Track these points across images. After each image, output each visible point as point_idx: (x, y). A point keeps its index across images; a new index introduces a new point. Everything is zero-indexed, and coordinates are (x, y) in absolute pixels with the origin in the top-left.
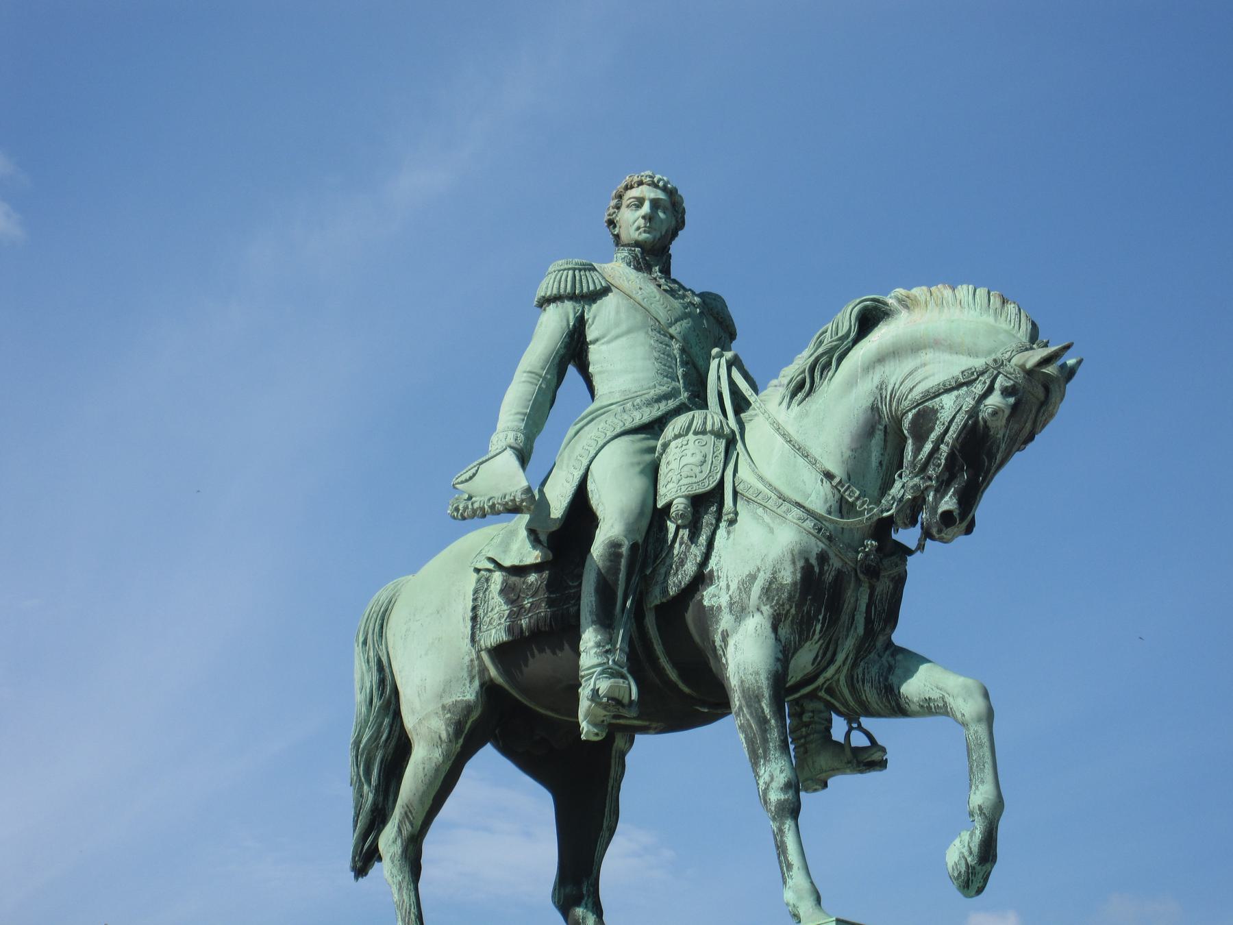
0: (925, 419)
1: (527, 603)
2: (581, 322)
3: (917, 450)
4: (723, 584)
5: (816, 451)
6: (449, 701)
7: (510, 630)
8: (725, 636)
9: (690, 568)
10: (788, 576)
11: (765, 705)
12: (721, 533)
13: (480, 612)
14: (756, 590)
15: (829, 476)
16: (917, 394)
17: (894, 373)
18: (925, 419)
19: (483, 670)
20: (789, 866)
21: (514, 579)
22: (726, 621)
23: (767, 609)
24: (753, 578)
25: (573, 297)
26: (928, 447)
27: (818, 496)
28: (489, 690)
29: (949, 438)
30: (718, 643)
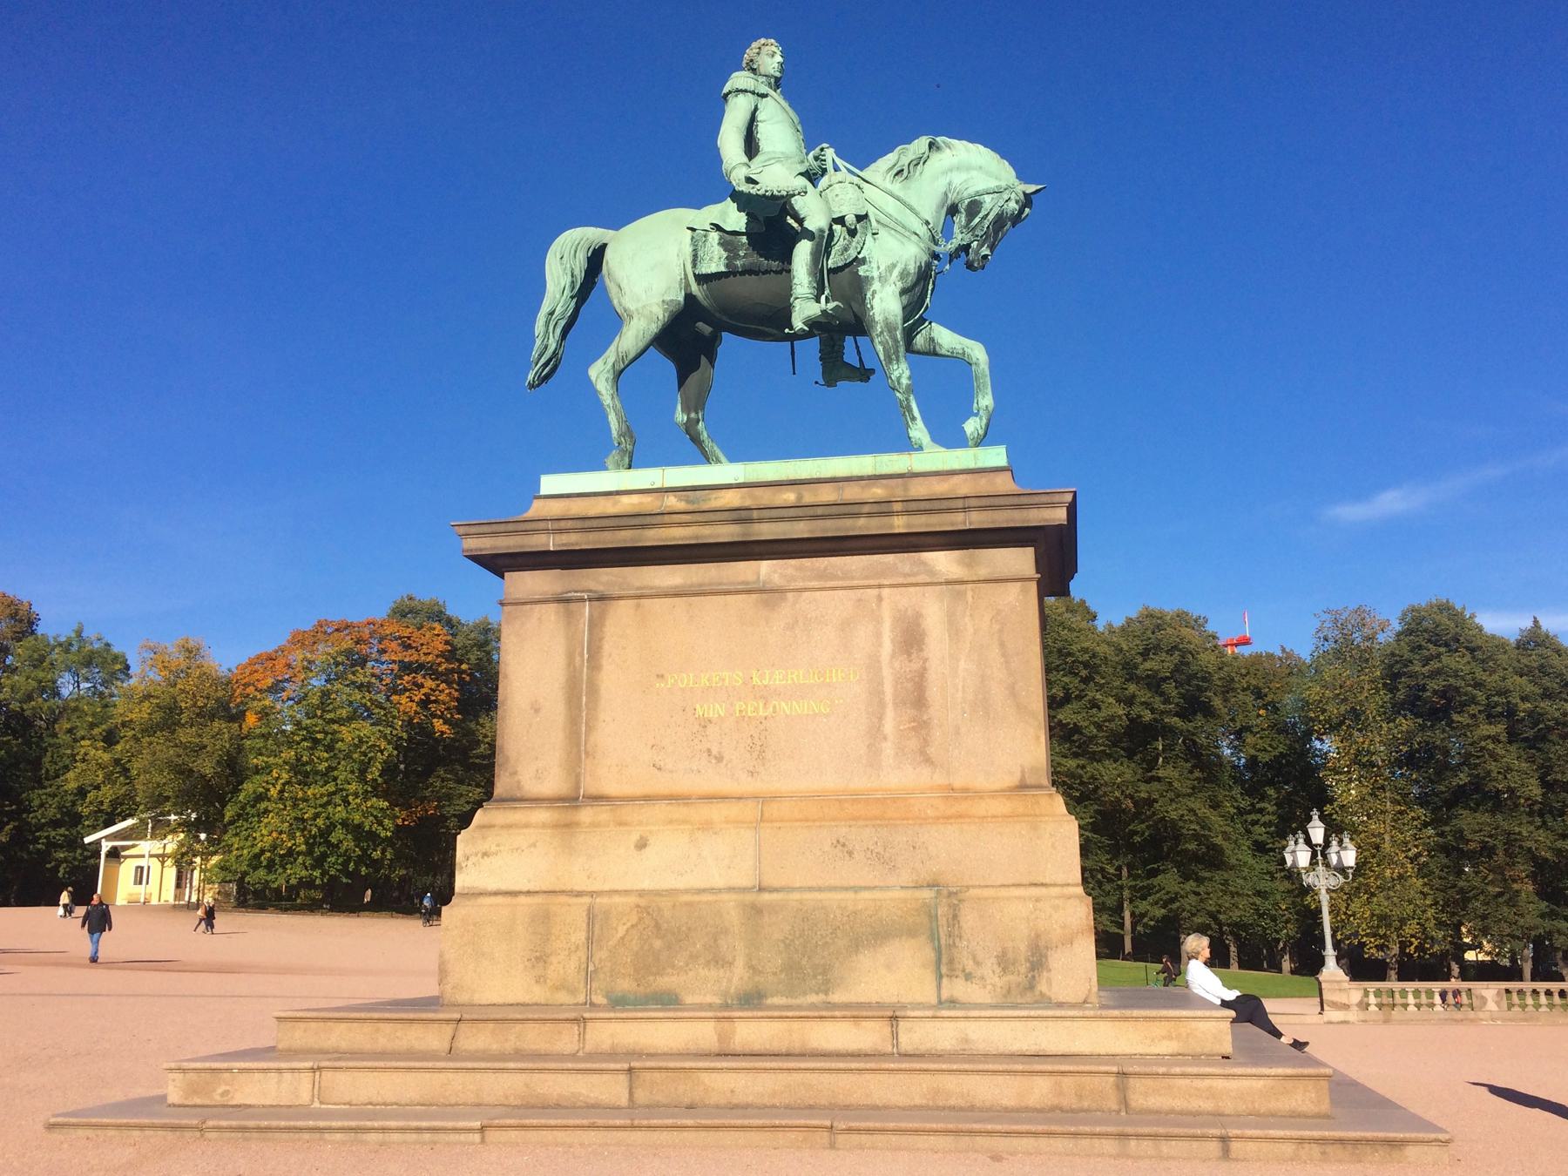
0: (974, 207)
1: (741, 253)
2: (756, 109)
3: (969, 221)
4: (874, 265)
5: (918, 208)
6: (668, 298)
7: (727, 266)
8: (874, 292)
9: (852, 253)
10: (912, 268)
11: (899, 335)
12: (869, 238)
13: (700, 253)
14: (896, 273)
15: (927, 223)
16: (971, 191)
17: (958, 179)
18: (974, 207)
19: (688, 285)
20: (913, 419)
21: (728, 237)
22: (876, 286)
23: (900, 285)
24: (894, 266)
25: (753, 93)
26: (977, 220)
27: (922, 230)
28: (689, 297)
29: (991, 217)
30: (869, 295)
